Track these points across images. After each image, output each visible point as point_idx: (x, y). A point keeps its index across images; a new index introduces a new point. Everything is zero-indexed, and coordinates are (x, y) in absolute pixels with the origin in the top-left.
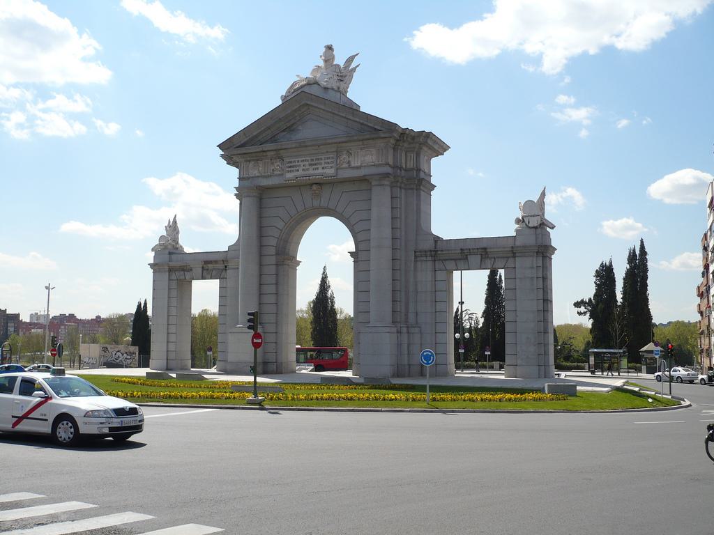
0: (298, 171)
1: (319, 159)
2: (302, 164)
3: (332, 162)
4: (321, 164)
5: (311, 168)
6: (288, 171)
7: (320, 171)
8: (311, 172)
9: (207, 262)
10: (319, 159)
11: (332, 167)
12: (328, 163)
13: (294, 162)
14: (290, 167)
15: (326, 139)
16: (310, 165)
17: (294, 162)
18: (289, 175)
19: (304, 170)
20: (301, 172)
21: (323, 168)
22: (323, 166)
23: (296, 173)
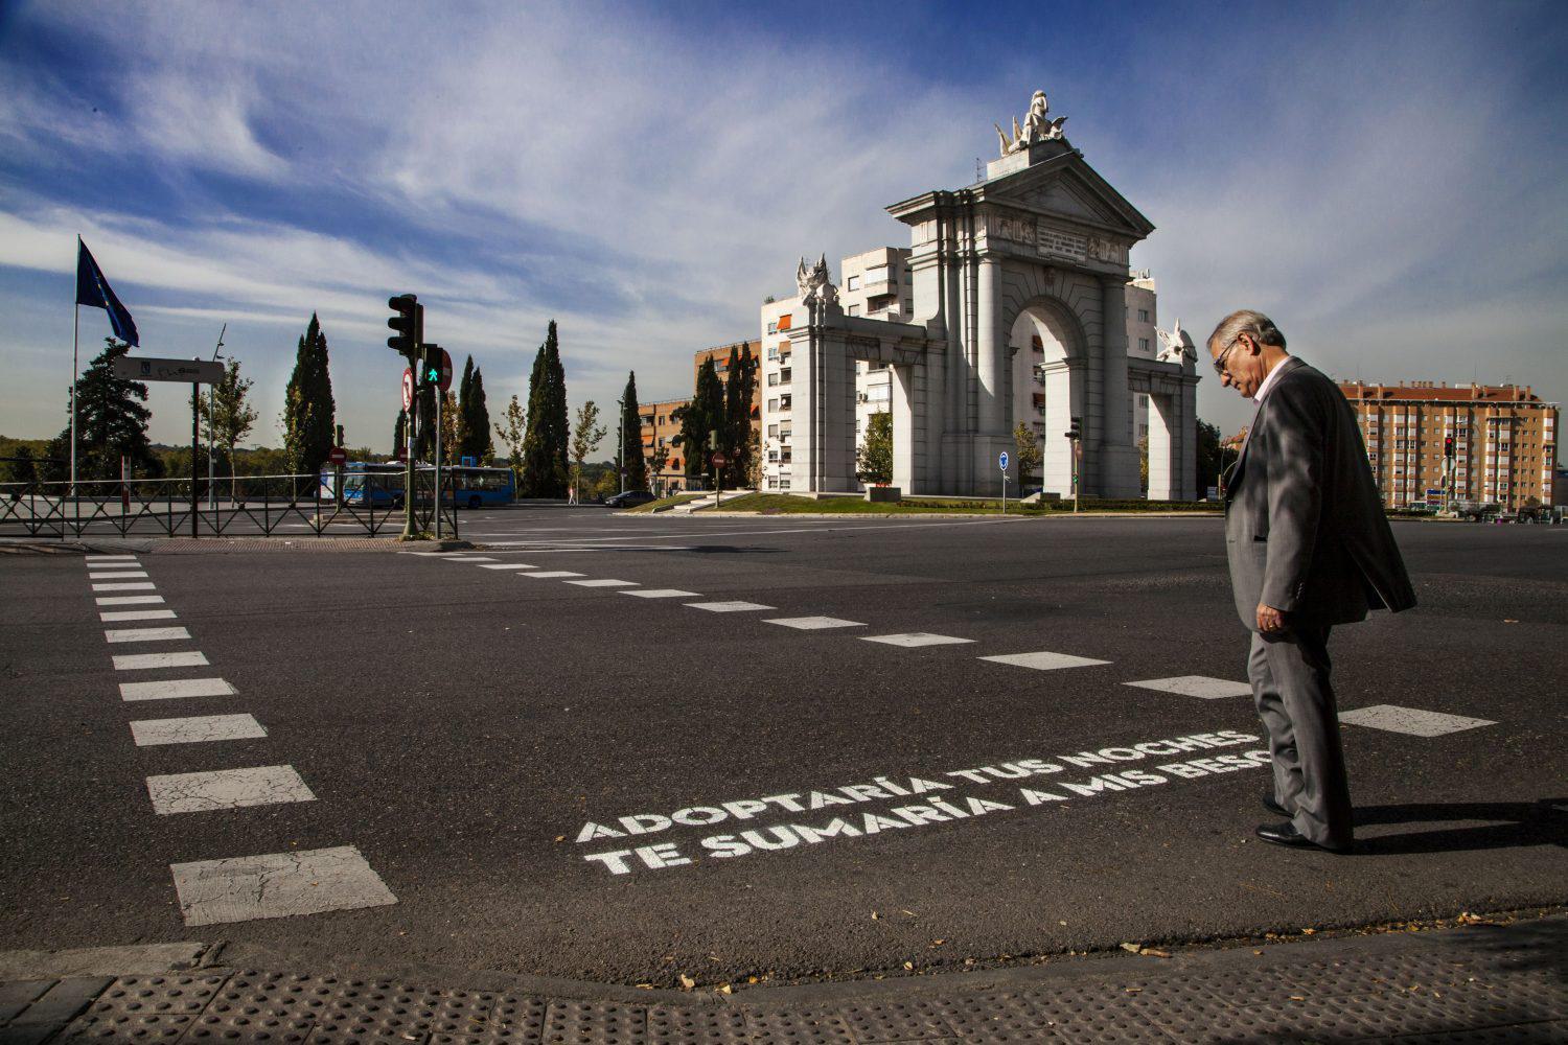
0: (1051, 247)
1: (1070, 240)
2: (1055, 240)
3: (1083, 248)
4: (1073, 246)
5: (1065, 248)
6: (1042, 245)
7: (1072, 255)
8: (1064, 253)
9: (904, 338)
10: (1070, 240)
11: (1083, 254)
12: (1079, 247)
13: (1047, 234)
14: (1043, 239)
15: (1071, 215)
16: (1063, 244)
17: (1047, 234)
18: (1043, 250)
19: (1057, 248)
20: (1054, 251)
21: (1076, 252)
22: (1075, 249)
23: (1051, 250)
